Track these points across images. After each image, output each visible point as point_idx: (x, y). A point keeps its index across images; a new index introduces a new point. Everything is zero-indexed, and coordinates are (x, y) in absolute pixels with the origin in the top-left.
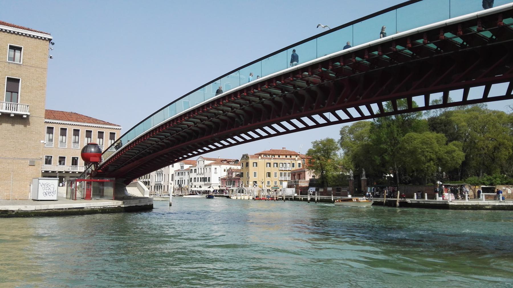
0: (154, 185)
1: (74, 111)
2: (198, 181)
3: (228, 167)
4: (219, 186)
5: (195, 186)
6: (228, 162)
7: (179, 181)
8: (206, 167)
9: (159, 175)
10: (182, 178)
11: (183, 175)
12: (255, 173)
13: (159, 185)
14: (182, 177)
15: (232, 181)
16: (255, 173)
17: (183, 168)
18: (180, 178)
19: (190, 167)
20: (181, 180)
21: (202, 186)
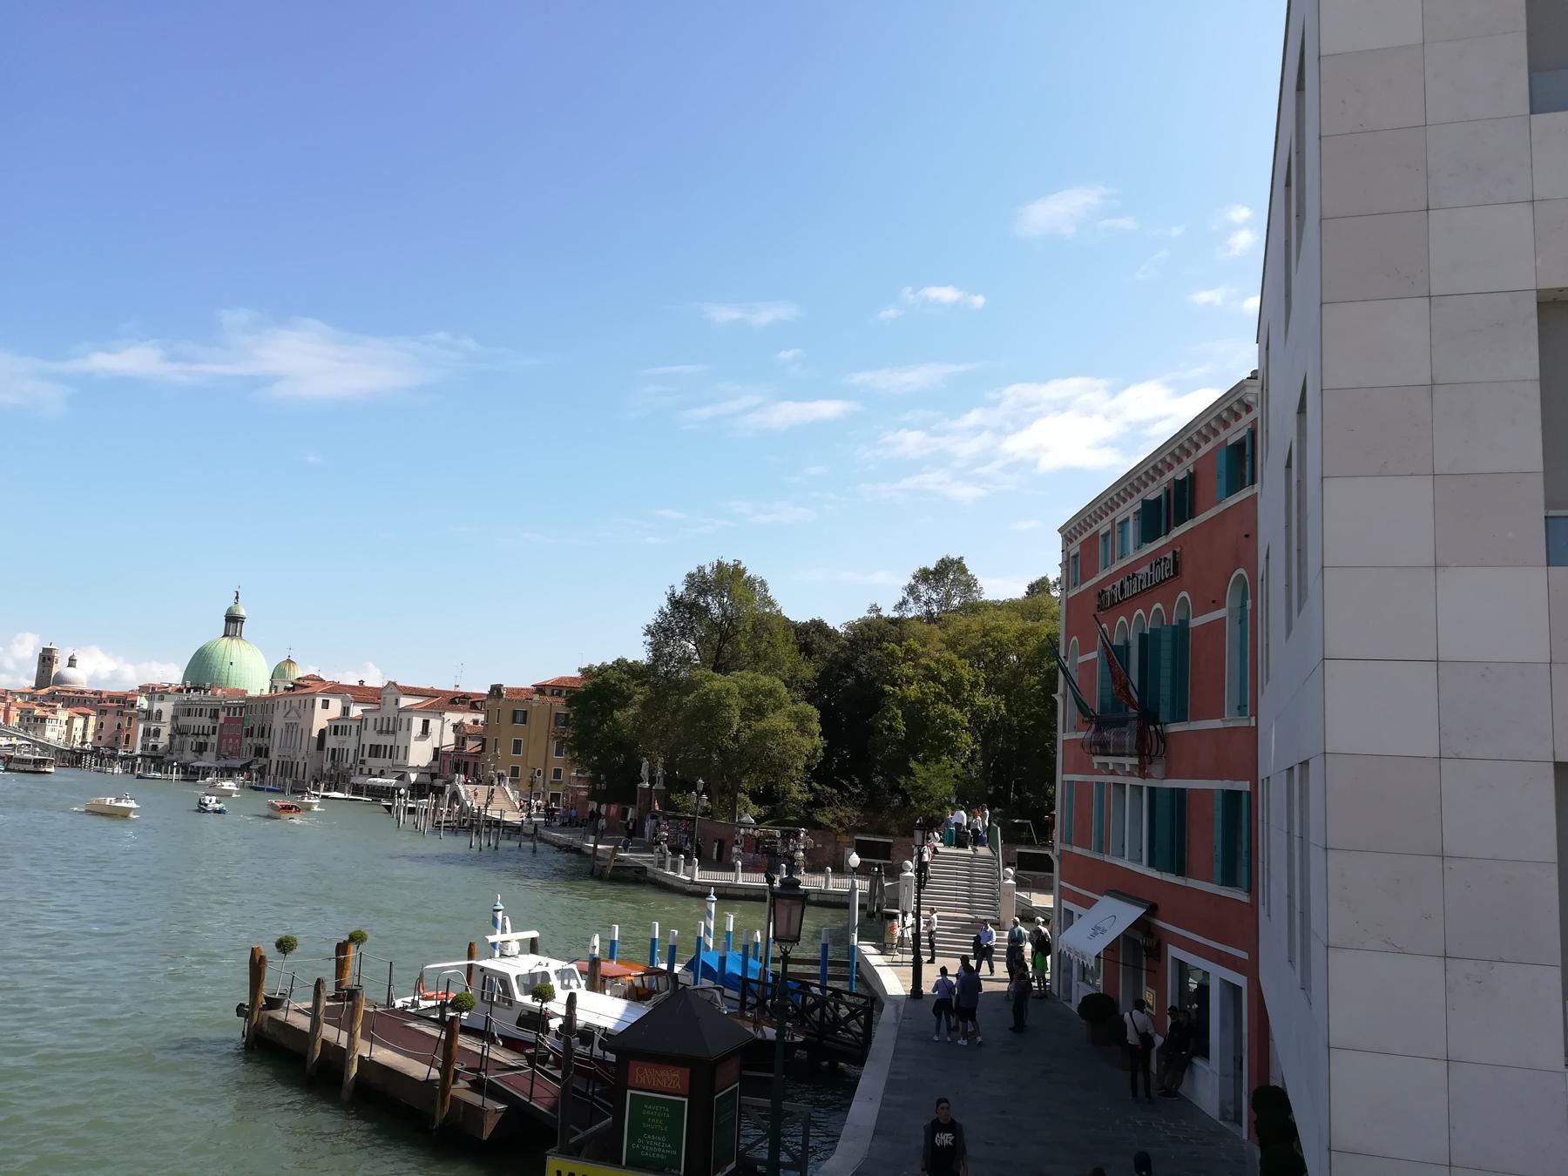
0: (277, 758)
3: (468, 718)
5: (370, 770)
7: (334, 750)
8: (403, 715)
11: (345, 734)
12: (517, 744)
13: (286, 759)
14: (344, 738)
16: (517, 744)
17: (348, 715)
19: (362, 710)
21: (385, 770)
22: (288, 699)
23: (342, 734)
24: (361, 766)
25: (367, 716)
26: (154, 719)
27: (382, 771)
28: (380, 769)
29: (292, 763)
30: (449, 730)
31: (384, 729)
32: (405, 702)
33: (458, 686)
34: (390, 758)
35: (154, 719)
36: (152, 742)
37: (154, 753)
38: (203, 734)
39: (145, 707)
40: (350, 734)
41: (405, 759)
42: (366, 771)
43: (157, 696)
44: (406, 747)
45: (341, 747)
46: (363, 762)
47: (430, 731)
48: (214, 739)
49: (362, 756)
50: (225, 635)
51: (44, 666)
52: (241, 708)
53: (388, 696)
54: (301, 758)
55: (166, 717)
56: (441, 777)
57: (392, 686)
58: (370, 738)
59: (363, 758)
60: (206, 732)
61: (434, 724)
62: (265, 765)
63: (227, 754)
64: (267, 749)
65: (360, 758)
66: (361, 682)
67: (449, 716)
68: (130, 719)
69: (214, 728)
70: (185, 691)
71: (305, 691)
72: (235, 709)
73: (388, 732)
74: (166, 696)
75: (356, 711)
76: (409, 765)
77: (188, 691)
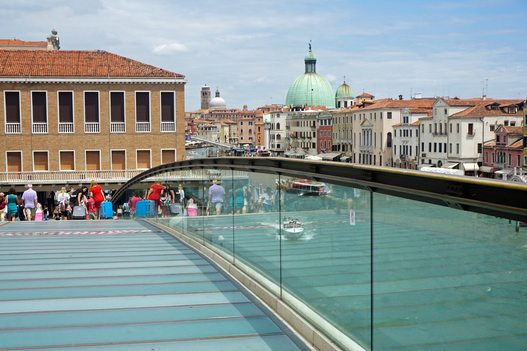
0: (359, 152)
1: (102, 49)
2: (435, 151)
3: (501, 120)
4: (480, 164)
5: (430, 161)
6: (502, 109)
9: (366, 133)
10: (407, 142)
11: (407, 136)
13: (366, 153)
14: (406, 138)
15: (504, 154)
17: (407, 122)
18: (404, 142)
19: (420, 119)
20: (404, 146)
21: (442, 161)
22: (362, 113)
23: (404, 136)
24: (423, 158)
25: (423, 122)
26: (276, 129)
27: (439, 162)
28: (438, 160)
29: (371, 156)
30: (487, 128)
31: (438, 131)
32: (452, 111)
33: (485, 96)
34: (445, 151)
35: (276, 129)
36: (276, 142)
37: (279, 150)
38: (307, 137)
39: (269, 120)
40: (411, 136)
41: (458, 152)
42: (427, 161)
43: (276, 114)
44: (458, 144)
45: (404, 145)
46: (424, 155)
47: (474, 131)
48: (314, 140)
49: (423, 150)
50: (307, 72)
51: (204, 98)
52: (329, 120)
53: (438, 108)
54: (376, 152)
55: (283, 127)
56: (486, 165)
57: (441, 101)
58: (427, 138)
59: (424, 152)
60: (309, 136)
61: (477, 126)
62: (351, 157)
63: (324, 149)
64: (351, 146)
65: (421, 153)
66: (401, 97)
67: (486, 119)
68: (259, 128)
69: (314, 133)
70: (291, 110)
71: (372, 107)
72: (325, 121)
73: (441, 134)
74: (281, 114)
75: (414, 119)
76: (462, 157)
77: (293, 110)
